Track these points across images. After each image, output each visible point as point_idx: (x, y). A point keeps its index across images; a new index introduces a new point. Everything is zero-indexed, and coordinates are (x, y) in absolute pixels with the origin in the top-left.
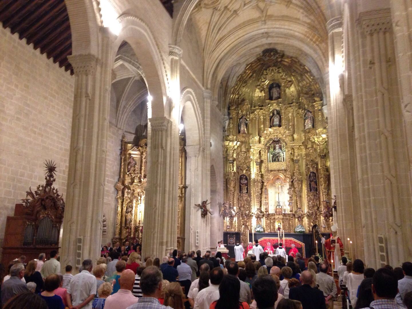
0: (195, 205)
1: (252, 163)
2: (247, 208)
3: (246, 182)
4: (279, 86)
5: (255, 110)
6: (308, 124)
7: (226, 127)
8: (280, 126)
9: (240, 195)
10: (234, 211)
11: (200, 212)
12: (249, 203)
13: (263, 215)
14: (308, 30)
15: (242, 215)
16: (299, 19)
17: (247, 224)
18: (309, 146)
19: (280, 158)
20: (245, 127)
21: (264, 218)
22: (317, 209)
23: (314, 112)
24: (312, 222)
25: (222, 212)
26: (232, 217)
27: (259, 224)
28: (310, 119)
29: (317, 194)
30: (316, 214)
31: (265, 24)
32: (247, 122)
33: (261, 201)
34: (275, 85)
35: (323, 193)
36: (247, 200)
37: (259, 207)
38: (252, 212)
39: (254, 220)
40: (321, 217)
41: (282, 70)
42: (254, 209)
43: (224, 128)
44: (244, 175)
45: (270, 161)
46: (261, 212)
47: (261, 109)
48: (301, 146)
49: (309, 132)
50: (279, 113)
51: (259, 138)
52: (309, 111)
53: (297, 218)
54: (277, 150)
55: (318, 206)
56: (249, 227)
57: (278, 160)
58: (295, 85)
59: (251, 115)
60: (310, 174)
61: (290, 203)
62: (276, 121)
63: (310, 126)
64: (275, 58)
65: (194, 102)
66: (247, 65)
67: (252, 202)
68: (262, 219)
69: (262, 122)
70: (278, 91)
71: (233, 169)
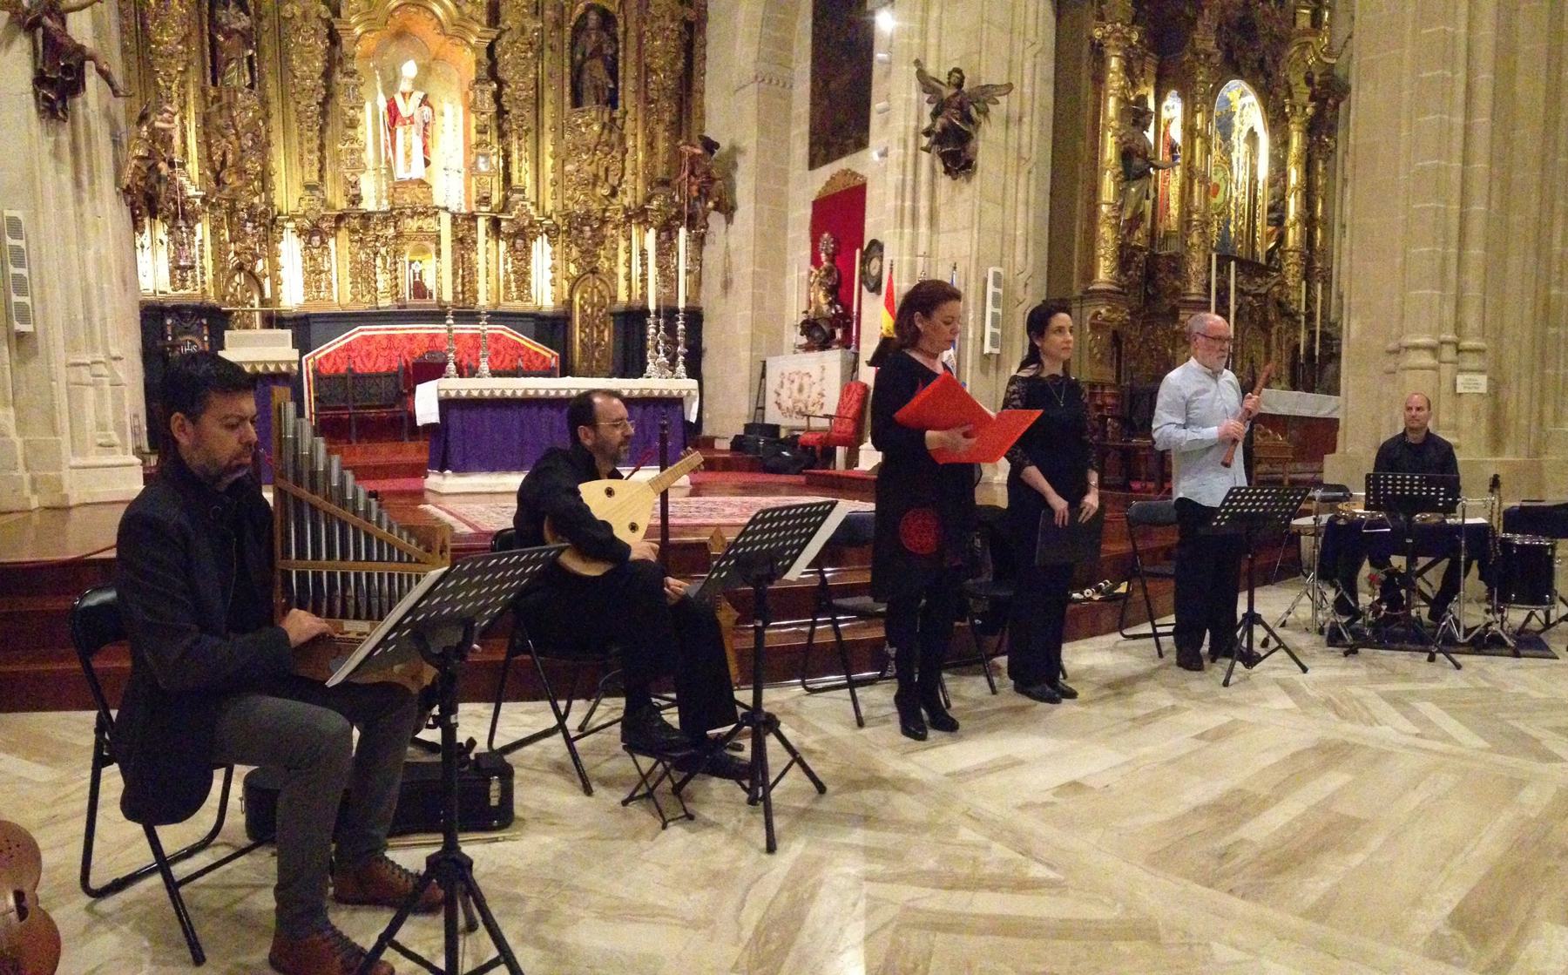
9: (218, 99)
13: (340, 218)
15: (232, 211)
17: (260, 266)
21: (343, 234)
27: (314, 274)
36: (252, 128)
39: (290, 248)
42: (287, 194)
53: (509, 236)
56: (267, 283)
68: (332, 242)
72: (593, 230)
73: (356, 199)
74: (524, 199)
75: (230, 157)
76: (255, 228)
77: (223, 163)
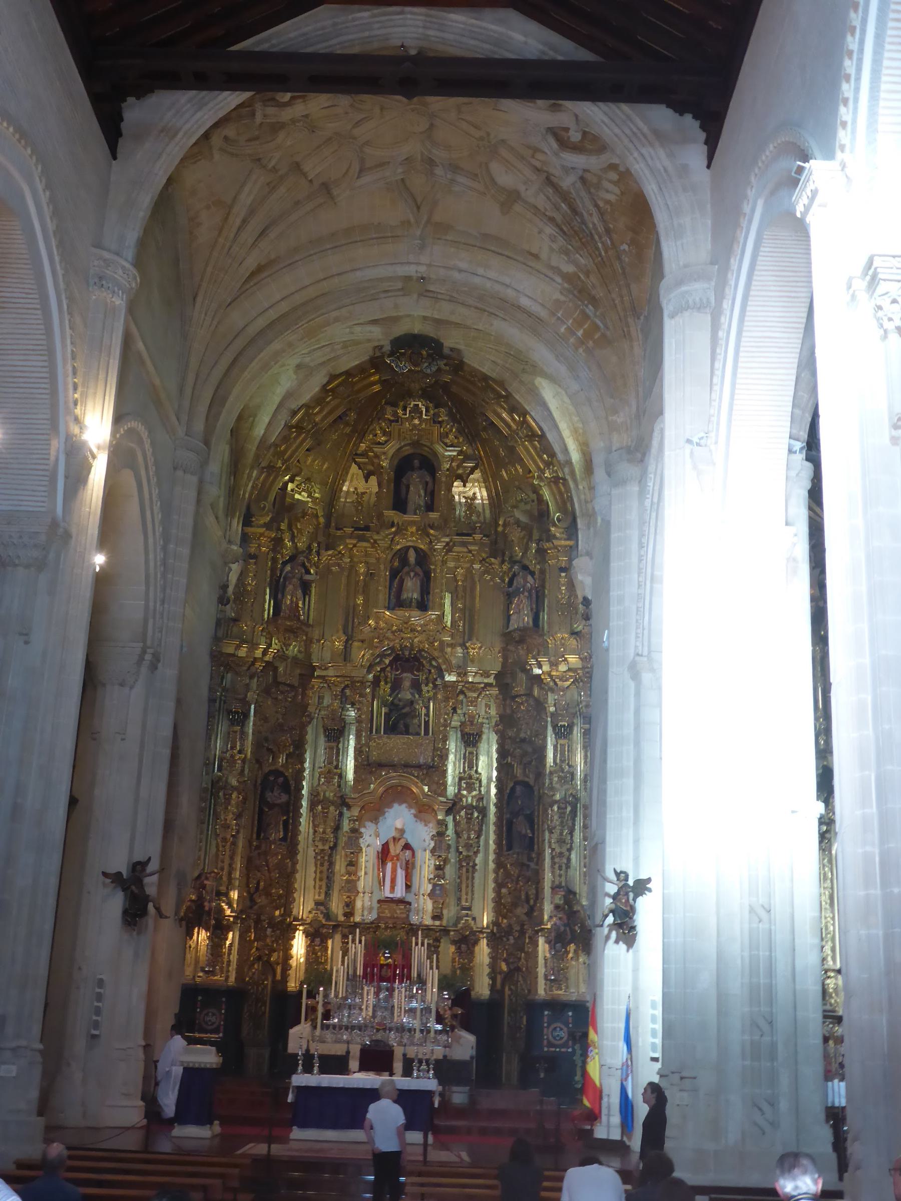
0: (105, 874)
1: (309, 729)
2: (280, 897)
3: (284, 798)
4: (429, 465)
5: (341, 538)
6: (518, 612)
7: (231, 589)
8: (423, 606)
9: (258, 847)
10: (230, 905)
11: (116, 903)
12: (287, 878)
13: (335, 927)
14: (562, 298)
15: (258, 921)
16: (536, 257)
18: (519, 689)
19: (416, 721)
20: (299, 593)
22: (526, 914)
23: (542, 572)
24: (505, 960)
25: (188, 908)
26: (219, 930)
28: (530, 597)
29: (530, 859)
30: (522, 932)
31: (422, 247)
32: (307, 577)
33: (333, 873)
34: (416, 463)
35: (553, 858)
37: (323, 896)
38: (295, 912)
40: (541, 941)
41: (451, 415)
43: (225, 587)
44: (278, 773)
45: (378, 731)
46: (328, 916)
47: (362, 539)
48: (490, 685)
49: (521, 641)
50: (423, 558)
51: (347, 642)
52: (525, 568)
53: (454, 942)
54: (406, 695)
55: (532, 902)
56: (279, 969)
57: (407, 727)
58: (484, 473)
59: (322, 552)
60: (513, 789)
61: (435, 885)
62: (411, 589)
63: (527, 620)
64: (434, 369)
65: (143, 473)
66: (333, 378)
67: (298, 876)
68: (330, 942)
69: (361, 584)
70: (427, 483)
71: (242, 745)
72: (515, 939)
73: (349, 914)
74: (467, 915)
75: (262, 884)
76: (273, 931)
77: (257, 888)
